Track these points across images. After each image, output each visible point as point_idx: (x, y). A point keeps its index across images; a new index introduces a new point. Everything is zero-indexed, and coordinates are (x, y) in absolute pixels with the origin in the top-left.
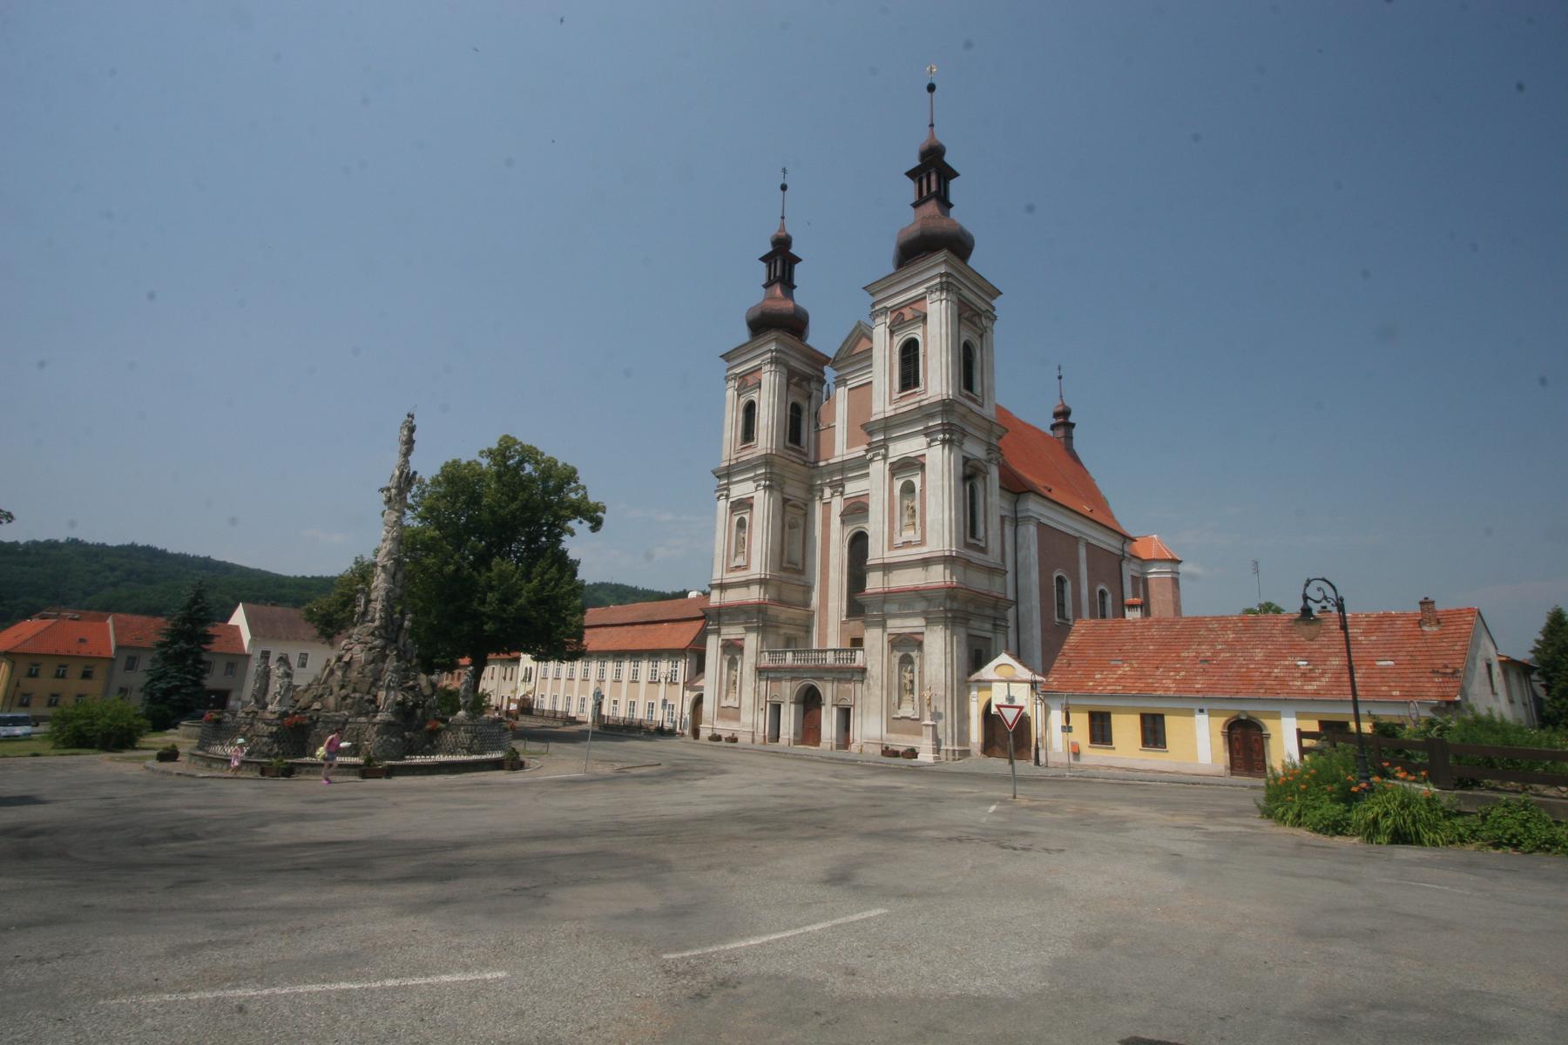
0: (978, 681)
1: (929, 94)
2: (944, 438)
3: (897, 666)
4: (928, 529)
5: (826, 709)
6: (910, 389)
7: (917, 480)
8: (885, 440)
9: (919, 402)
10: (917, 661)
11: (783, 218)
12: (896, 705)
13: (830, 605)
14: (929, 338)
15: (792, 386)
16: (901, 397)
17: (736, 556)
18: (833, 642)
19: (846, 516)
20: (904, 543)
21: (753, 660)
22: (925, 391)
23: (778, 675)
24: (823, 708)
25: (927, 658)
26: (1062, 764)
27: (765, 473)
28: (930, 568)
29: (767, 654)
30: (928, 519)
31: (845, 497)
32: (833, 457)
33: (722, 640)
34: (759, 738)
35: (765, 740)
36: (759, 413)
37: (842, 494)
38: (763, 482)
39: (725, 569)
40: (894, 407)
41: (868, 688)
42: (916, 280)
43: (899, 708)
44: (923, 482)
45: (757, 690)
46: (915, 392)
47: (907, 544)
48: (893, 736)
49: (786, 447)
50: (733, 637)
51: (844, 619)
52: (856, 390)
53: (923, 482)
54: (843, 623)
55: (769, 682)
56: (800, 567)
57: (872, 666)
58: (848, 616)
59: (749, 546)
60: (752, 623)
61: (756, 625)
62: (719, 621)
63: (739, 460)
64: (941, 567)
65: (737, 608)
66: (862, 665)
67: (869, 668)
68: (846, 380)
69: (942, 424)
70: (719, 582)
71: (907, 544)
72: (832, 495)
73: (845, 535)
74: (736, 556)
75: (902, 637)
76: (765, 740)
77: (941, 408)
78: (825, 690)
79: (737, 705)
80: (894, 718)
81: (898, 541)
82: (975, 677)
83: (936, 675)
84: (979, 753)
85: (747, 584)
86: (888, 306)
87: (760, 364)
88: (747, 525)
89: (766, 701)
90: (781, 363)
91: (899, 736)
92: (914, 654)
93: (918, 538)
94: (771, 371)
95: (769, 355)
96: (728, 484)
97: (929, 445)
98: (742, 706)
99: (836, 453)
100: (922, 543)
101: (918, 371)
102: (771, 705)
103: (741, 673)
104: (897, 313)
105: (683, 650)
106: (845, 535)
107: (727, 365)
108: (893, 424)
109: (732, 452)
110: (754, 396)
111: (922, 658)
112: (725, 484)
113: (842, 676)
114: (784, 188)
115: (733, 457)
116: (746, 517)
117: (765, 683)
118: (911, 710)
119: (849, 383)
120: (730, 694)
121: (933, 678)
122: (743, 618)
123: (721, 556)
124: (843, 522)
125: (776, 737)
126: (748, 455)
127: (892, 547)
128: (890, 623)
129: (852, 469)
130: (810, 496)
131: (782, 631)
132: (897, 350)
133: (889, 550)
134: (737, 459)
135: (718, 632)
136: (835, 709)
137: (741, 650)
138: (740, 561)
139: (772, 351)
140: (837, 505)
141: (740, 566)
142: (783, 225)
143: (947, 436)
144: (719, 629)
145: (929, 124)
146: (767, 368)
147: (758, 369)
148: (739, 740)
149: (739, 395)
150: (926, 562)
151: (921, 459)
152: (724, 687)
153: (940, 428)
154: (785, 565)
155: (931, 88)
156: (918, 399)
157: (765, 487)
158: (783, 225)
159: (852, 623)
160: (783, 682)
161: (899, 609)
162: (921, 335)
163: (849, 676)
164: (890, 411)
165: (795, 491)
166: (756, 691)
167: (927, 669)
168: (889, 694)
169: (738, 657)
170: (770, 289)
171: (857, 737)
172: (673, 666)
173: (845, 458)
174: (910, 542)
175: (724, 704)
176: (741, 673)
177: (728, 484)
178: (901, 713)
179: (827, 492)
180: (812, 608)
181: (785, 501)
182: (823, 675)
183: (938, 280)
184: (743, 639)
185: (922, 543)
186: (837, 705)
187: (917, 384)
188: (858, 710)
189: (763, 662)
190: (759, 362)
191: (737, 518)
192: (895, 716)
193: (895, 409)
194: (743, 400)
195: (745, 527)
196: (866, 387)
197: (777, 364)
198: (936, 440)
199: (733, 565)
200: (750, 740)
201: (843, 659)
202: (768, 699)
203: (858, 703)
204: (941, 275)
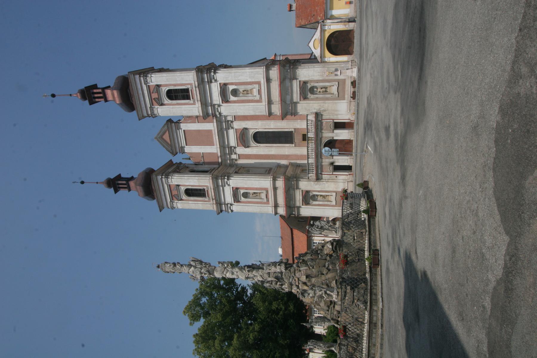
0: (321, 57)
1: (56, 97)
2: (213, 72)
3: (315, 96)
4: (253, 80)
5: (337, 136)
6: (189, 95)
7: (231, 87)
8: (211, 106)
9: (196, 87)
10: (313, 84)
11: (97, 183)
12: (332, 95)
13: (287, 153)
14: (167, 83)
15: (180, 171)
16: (193, 98)
17: (261, 199)
18: (303, 151)
19: (247, 146)
20: (259, 94)
21: (312, 183)
22: (191, 84)
23: (320, 167)
24: (335, 138)
25: (310, 78)
26: (355, 9)
27: (221, 179)
28: (271, 78)
29: (309, 175)
30: (249, 80)
31: (236, 146)
32: (217, 153)
33: (303, 205)
34: (350, 178)
35: (351, 174)
36: (191, 186)
37: (235, 148)
38: (226, 180)
39: (267, 205)
40: (196, 102)
41: (325, 111)
42: (140, 92)
43: (333, 94)
44: (232, 84)
45: (327, 180)
46: (191, 90)
47: (259, 92)
48: (346, 96)
49: (210, 173)
50: (301, 198)
51: (293, 145)
52: (187, 141)
53: (232, 84)
54: (295, 146)
55: (323, 173)
56: (269, 169)
57: (315, 109)
58: (292, 143)
59: (257, 189)
60: (294, 184)
61: (295, 182)
62: (293, 207)
63: (214, 198)
64: (271, 72)
65: (287, 193)
66: (314, 115)
67: (315, 111)
68: (182, 147)
69: (207, 73)
70: (273, 208)
71: (259, 92)
72: (235, 153)
73: (254, 145)
74: (261, 199)
75: (302, 93)
76: (351, 174)
77: (200, 73)
78: (326, 137)
79: (334, 194)
80: (338, 97)
81: (258, 98)
82: (319, 59)
83: (318, 72)
84: (352, 56)
85: (275, 189)
86: (149, 106)
87: (167, 184)
88: (246, 191)
89: (332, 174)
90: (168, 174)
91: (346, 93)
92: (309, 86)
93: (257, 86)
94: (172, 178)
95: (163, 179)
96: (225, 204)
97: (216, 81)
98: (335, 190)
99: (216, 152)
100: (259, 83)
101: (181, 89)
102: (334, 171)
103: (319, 192)
104: (153, 101)
105: (307, 237)
106: (254, 145)
107: (165, 209)
108: (204, 102)
109: (210, 203)
110: (183, 189)
111: (312, 81)
112: (225, 206)
113: (319, 127)
114: (82, 183)
115: (211, 202)
116: (242, 191)
117: (323, 175)
118: (334, 87)
119: (183, 146)
120: (330, 199)
121: (320, 74)
122: (292, 192)
123: (261, 207)
124: (248, 147)
125: (348, 168)
126: (211, 193)
127: (260, 101)
128: (295, 100)
129: (224, 142)
130: (235, 166)
131: (299, 173)
132: (170, 102)
133: (261, 102)
134: (213, 199)
135: (299, 208)
136: (336, 131)
137: (307, 192)
138: (263, 196)
139: (162, 178)
140: (241, 150)
141: (266, 195)
142: (101, 183)
143: (213, 71)
144: (297, 207)
145: (70, 97)
146: (169, 180)
147: (169, 186)
148: (352, 191)
149: (181, 200)
150: (268, 80)
151: (221, 85)
152: (326, 203)
153: (208, 74)
154: (267, 173)
155: (53, 96)
156: (194, 88)
157: (228, 179)
158: (101, 183)
159: (295, 141)
160: (323, 164)
161: (289, 95)
162: (165, 88)
163: (319, 123)
164: (198, 105)
165: (232, 170)
166: (328, 181)
167: (316, 78)
168: (327, 99)
169: (311, 194)
170: (132, 188)
171: (347, 117)
172: (316, 313)
173: (218, 146)
174: (259, 90)
175: (334, 203)
176: (319, 192)
177: (225, 204)
178: (336, 93)
179: (234, 156)
180: (288, 164)
181: (236, 173)
182: (319, 139)
183: (142, 78)
184: (302, 191)
185: (259, 83)
186: (333, 130)
187: (187, 90)
188: (335, 117)
189: (313, 177)
190: (166, 185)
191: (242, 198)
192: (337, 96)
193: (198, 101)
194: (184, 197)
195: (247, 193)
196: (186, 132)
197: (168, 176)
198: (213, 76)
199: (265, 200)
200: (351, 183)
201: (312, 166)
202: (331, 173)
203: (332, 117)
204: (140, 77)
